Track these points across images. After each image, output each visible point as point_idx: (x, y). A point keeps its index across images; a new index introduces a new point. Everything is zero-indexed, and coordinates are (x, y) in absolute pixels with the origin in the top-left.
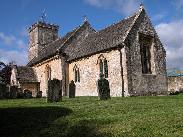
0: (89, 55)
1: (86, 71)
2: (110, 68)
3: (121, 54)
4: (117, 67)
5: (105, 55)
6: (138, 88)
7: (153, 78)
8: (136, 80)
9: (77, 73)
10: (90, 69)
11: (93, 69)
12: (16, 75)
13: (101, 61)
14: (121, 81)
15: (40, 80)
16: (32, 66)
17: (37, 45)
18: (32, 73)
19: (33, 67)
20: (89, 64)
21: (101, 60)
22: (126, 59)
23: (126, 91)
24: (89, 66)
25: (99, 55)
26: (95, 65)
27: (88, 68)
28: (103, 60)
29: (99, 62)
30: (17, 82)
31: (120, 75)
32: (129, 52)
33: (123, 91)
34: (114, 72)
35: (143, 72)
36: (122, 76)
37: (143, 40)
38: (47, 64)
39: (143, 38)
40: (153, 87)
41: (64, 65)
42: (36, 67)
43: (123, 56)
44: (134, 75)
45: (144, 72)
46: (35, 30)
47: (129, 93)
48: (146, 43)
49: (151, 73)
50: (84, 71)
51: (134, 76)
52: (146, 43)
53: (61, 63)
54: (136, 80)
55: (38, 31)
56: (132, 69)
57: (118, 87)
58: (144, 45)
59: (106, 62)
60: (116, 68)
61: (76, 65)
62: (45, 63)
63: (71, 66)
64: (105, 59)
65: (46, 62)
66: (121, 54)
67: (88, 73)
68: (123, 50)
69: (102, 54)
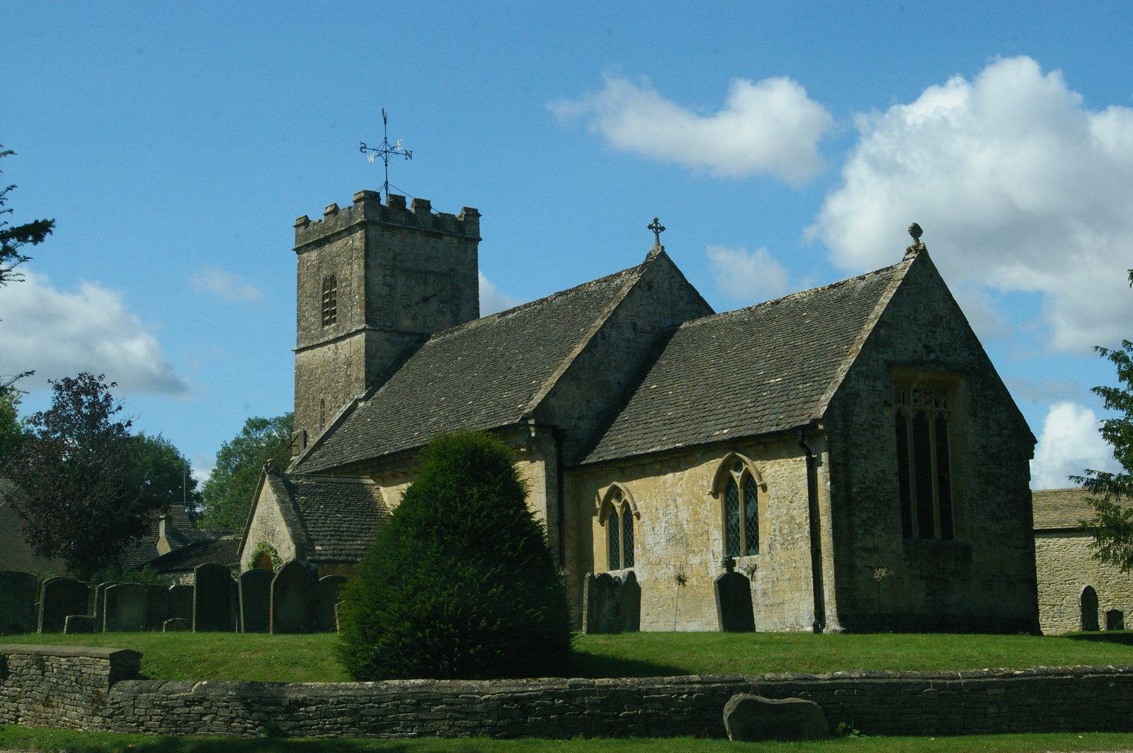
4: (795, 513)
10: (684, 515)
11: (696, 513)
14: (811, 572)
20: (679, 491)
22: (829, 483)
23: (830, 611)
24: (679, 501)
27: (672, 509)
28: (737, 476)
31: (805, 547)
34: (785, 531)
35: (907, 533)
37: (915, 391)
39: (914, 386)
43: (822, 472)
47: (842, 618)
50: (655, 519)
55: (367, 256)
57: (798, 594)
58: (920, 416)
60: (792, 518)
67: (673, 530)
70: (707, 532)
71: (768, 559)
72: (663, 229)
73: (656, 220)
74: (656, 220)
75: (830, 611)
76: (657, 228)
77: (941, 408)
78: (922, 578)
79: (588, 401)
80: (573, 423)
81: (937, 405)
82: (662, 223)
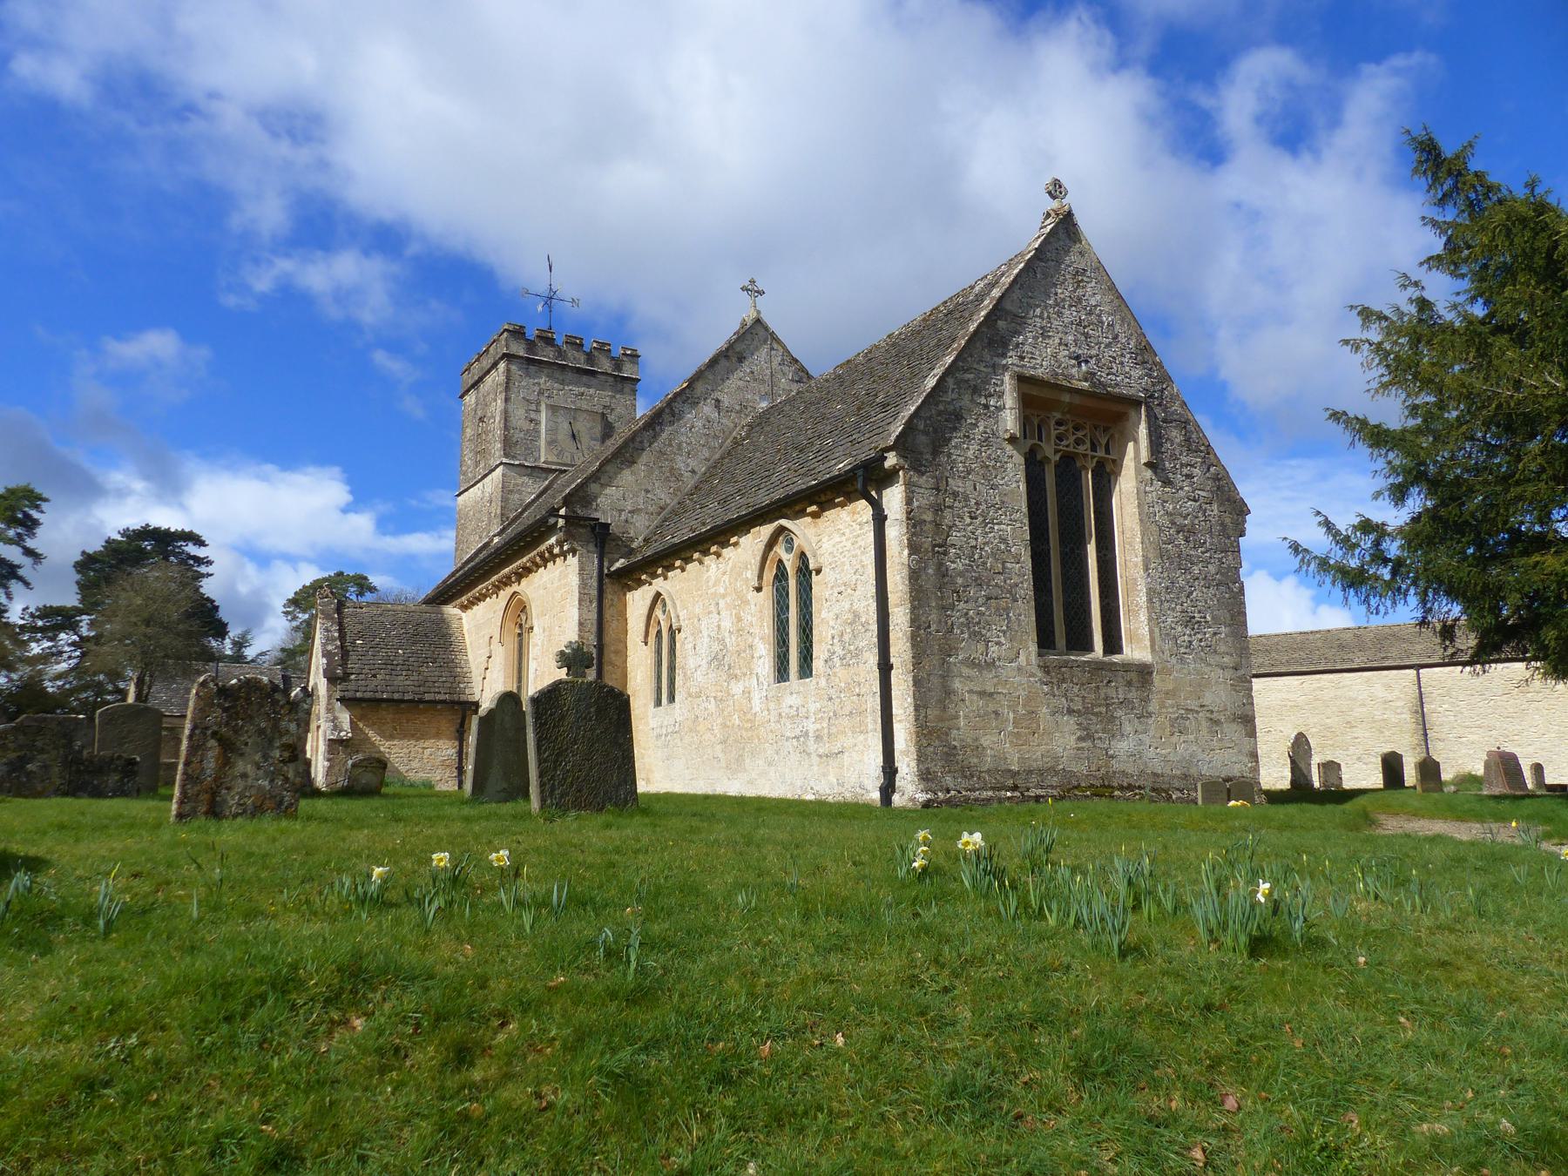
0: (720, 536)
1: (705, 633)
2: (824, 614)
3: (880, 519)
5: (803, 529)
6: (1000, 747)
7: (1129, 684)
8: (982, 694)
9: (666, 642)
10: (727, 624)
11: (739, 619)
12: (326, 654)
13: (781, 575)
15: (477, 691)
16: (446, 602)
17: (500, 470)
18: (438, 644)
19: (451, 610)
20: (722, 591)
21: (780, 561)
22: (906, 552)
23: (906, 766)
24: (722, 603)
25: (766, 531)
26: (752, 595)
29: (769, 575)
30: (330, 697)
31: (872, 659)
32: (938, 509)
33: (890, 770)
34: (846, 638)
35: (1045, 641)
36: (885, 668)
37: (1059, 423)
38: (509, 591)
39: (1058, 416)
40: (1122, 747)
41: (595, 592)
42: (464, 608)
43: (895, 533)
44: (972, 664)
45: (1061, 641)
46: (489, 380)
47: (925, 776)
48: (1081, 449)
49: (1113, 643)
51: (966, 671)
52: (1081, 449)
53: (574, 580)
54: (982, 694)
55: (507, 389)
56: (956, 617)
57: (862, 737)
59: (805, 572)
61: (658, 595)
62: (498, 588)
63: (637, 601)
64: (803, 556)
65: (506, 582)
66: (880, 519)
67: (716, 647)
68: (894, 498)
69: (783, 522)
70: (751, 647)
71: (823, 682)
72: (761, 293)
73: (752, 282)
74: (752, 282)
75: (906, 766)
76: (753, 290)
77: (1101, 453)
78: (1070, 712)
79: (647, 491)
80: (623, 517)
81: (1094, 448)
82: (760, 286)
